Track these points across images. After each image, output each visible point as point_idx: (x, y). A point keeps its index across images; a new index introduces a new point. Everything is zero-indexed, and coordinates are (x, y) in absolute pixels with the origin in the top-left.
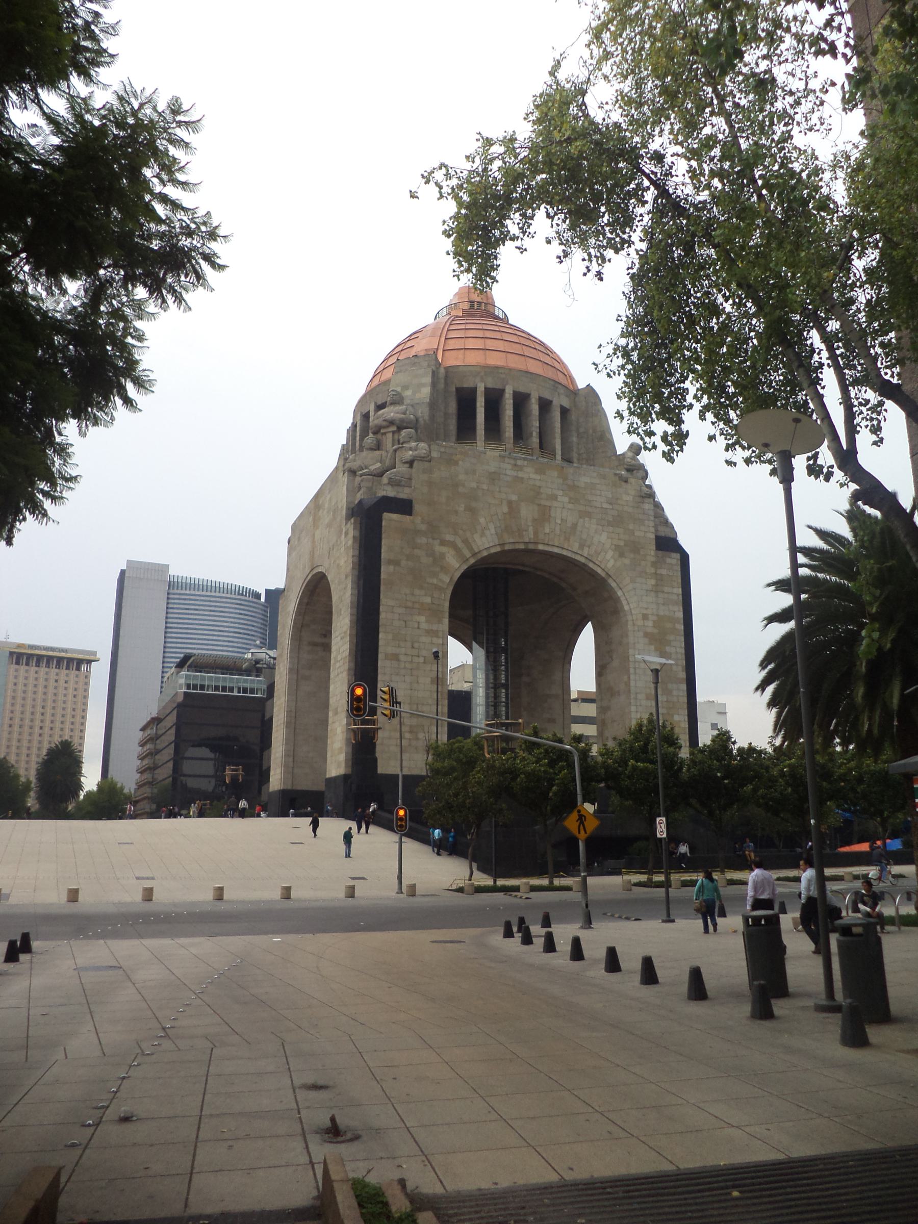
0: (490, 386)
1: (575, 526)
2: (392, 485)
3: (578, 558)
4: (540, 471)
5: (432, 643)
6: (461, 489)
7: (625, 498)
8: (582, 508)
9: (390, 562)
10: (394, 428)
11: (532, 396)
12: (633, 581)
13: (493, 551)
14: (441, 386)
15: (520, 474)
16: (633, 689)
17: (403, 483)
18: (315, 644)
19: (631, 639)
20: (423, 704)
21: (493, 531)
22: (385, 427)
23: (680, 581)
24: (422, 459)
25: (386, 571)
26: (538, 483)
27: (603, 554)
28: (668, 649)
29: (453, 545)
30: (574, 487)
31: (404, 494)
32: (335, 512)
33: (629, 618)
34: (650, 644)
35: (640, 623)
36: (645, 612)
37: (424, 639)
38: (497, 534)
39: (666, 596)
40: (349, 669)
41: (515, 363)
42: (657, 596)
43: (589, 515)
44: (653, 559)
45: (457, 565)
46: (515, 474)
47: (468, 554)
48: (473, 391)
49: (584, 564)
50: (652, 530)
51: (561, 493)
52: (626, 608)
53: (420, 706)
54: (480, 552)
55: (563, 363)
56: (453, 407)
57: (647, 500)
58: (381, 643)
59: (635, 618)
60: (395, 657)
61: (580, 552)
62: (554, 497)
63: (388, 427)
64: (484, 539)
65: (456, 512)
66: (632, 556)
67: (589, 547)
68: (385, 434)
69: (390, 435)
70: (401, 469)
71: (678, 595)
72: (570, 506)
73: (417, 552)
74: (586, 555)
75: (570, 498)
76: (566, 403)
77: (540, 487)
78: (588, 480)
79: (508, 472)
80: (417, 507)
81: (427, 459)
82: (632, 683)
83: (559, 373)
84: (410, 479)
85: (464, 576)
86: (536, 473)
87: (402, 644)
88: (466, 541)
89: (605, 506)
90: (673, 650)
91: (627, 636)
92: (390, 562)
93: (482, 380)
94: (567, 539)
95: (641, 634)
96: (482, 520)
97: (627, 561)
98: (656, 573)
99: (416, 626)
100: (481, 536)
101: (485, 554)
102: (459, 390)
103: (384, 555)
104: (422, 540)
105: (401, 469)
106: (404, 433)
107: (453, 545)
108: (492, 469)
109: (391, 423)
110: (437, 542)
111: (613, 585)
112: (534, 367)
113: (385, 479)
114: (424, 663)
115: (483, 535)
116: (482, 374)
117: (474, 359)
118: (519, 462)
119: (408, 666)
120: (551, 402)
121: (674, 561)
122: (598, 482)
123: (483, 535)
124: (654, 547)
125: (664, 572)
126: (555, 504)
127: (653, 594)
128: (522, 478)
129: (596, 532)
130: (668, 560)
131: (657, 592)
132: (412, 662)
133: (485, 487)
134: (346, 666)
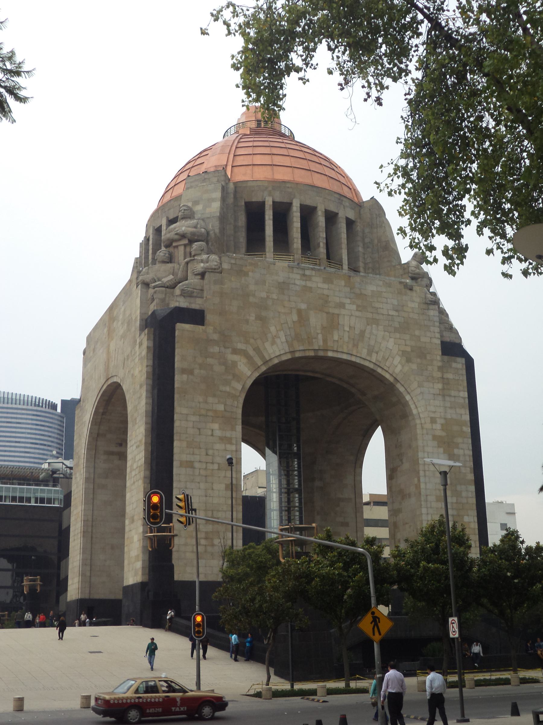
0: (277, 200)
1: (362, 333)
2: (184, 296)
3: (367, 364)
4: (328, 280)
5: (226, 450)
6: (251, 299)
7: (411, 305)
8: (370, 315)
9: (184, 371)
10: (186, 241)
11: (319, 208)
12: (420, 385)
13: (284, 358)
14: (231, 200)
15: (309, 284)
16: (423, 492)
17: (195, 294)
18: (112, 453)
19: (420, 443)
20: (218, 511)
21: (283, 339)
22: (176, 241)
23: (465, 384)
24: (213, 270)
25: (179, 379)
26: (326, 292)
27: (390, 359)
28: (456, 451)
30: (361, 296)
31: (196, 304)
32: (129, 324)
33: (418, 421)
34: (439, 447)
35: (428, 426)
36: (433, 415)
37: (218, 446)
38: (287, 341)
39: (453, 399)
40: (145, 477)
41: (301, 177)
42: (444, 400)
43: (376, 322)
44: (440, 364)
45: (249, 373)
46: (303, 283)
47: (260, 363)
48: (262, 205)
49: (372, 370)
50: (438, 335)
51: (348, 301)
52: (415, 412)
53: (215, 513)
54: (271, 359)
55: (348, 177)
56: (242, 220)
57: (431, 307)
58: (176, 450)
59: (423, 422)
60: (190, 465)
61: (368, 358)
62: (342, 305)
64: (275, 347)
65: (247, 321)
66: (419, 360)
67: (377, 353)
68: (177, 247)
69: (182, 249)
70: (193, 280)
72: (358, 314)
73: (210, 360)
74: (374, 361)
75: (358, 306)
76: (351, 215)
77: (328, 296)
78: (374, 288)
79: (298, 282)
80: (209, 317)
81: (217, 270)
82: (422, 486)
83: (343, 186)
84: (202, 290)
85: (256, 383)
86: (324, 282)
87: (197, 451)
88: (257, 350)
89: (392, 313)
90: (461, 452)
91: (416, 439)
92: (184, 371)
93: (270, 195)
94: (356, 346)
95: (430, 437)
96: (273, 329)
97: (414, 367)
98: (443, 378)
99: (210, 433)
101: (276, 361)
102: (246, 203)
103: (178, 365)
104: (216, 349)
105: (193, 280)
106: (195, 245)
108: (281, 279)
109: (183, 236)
110: (229, 351)
111: (402, 389)
112: (319, 181)
113: (177, 291)
114: (219, 469)
115: (273, 343)
116: (270, 189)
117: (261, 174)
118: (308, 272)
119: (203, 472)
120: (337, 214)
121: (459, 366)
122: (384, 290)
123: (273, 343)
124: (440, 353)
125: (450, 376)
126: (343, 312)
127: (440, 398)
128: (311, 288)
129: (383, 338)
130: (454, 365)
131: (444, 396)
133: (275, 296)
134: (142, 474)
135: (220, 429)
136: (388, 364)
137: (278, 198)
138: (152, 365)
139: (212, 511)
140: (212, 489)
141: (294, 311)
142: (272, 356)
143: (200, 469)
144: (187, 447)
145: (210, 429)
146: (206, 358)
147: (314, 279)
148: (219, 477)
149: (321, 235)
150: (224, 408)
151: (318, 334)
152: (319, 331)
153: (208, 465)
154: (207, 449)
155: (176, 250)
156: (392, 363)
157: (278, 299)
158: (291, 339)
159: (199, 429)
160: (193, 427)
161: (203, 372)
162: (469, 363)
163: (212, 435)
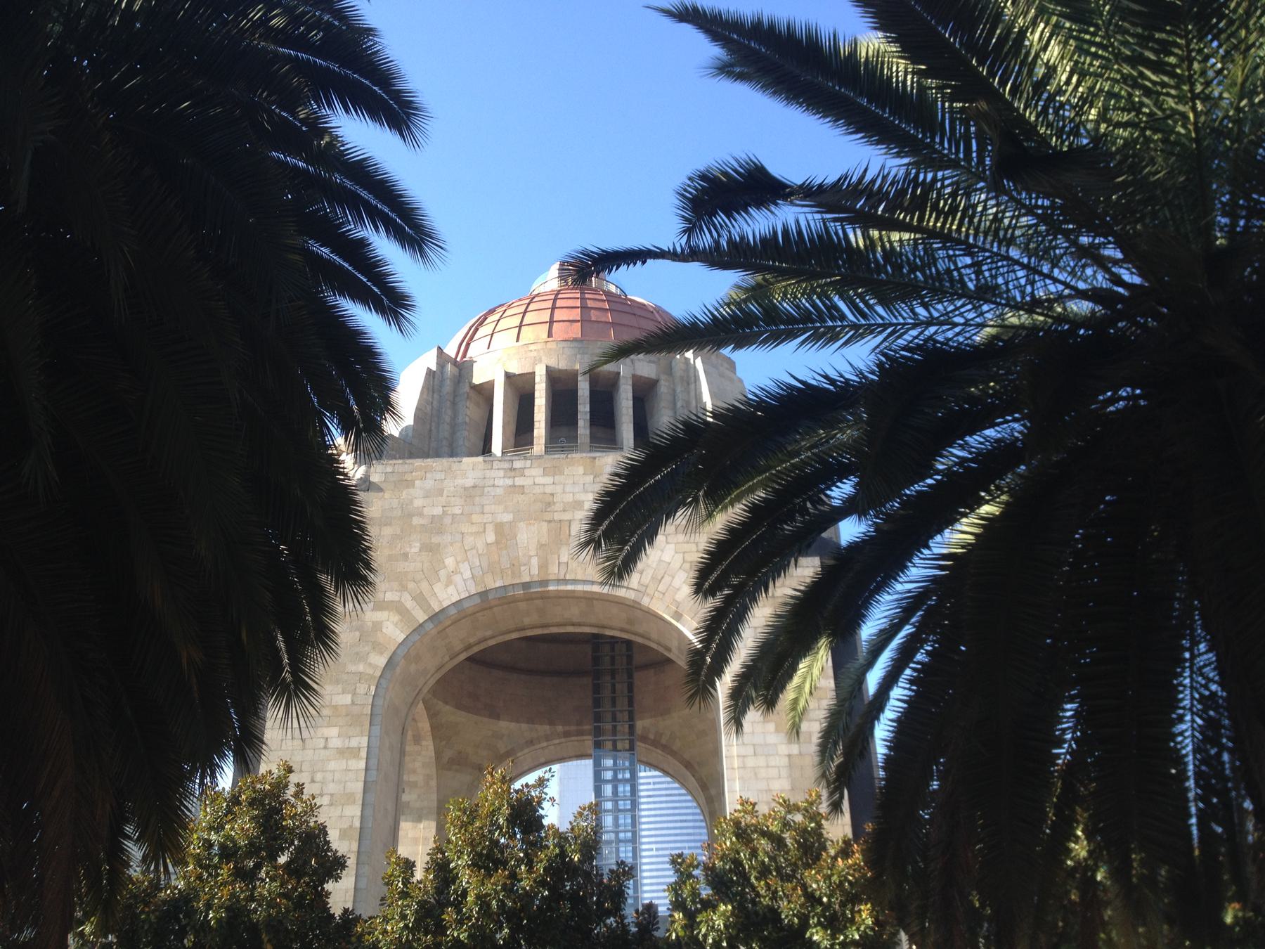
6: (416, 521)
15: (519, 481)
21: (467, 574)
26: (549, 490)
27: (667, 579)
29: (398, 608)
46: (509, 482)
64: (451, 590)
65: (405, 556)
79: (500, 482)
86: (545, 475)
88: (420, 599)
96: (450, 562)
99: (322, 745)
100: (447, 586)
108: (469, 482)
114: (331, 804)
115: (449, 582)
133: (457, 511)
136: (661, 588)
137: (516, 369)
141: (490, 528)
142: (445, 604)
147: (527, 472)
149: (584, 408)
152: (533, 553)
156: (670, 585)
157: (462, 514)
158: (481, 573)
163: (325, 748)
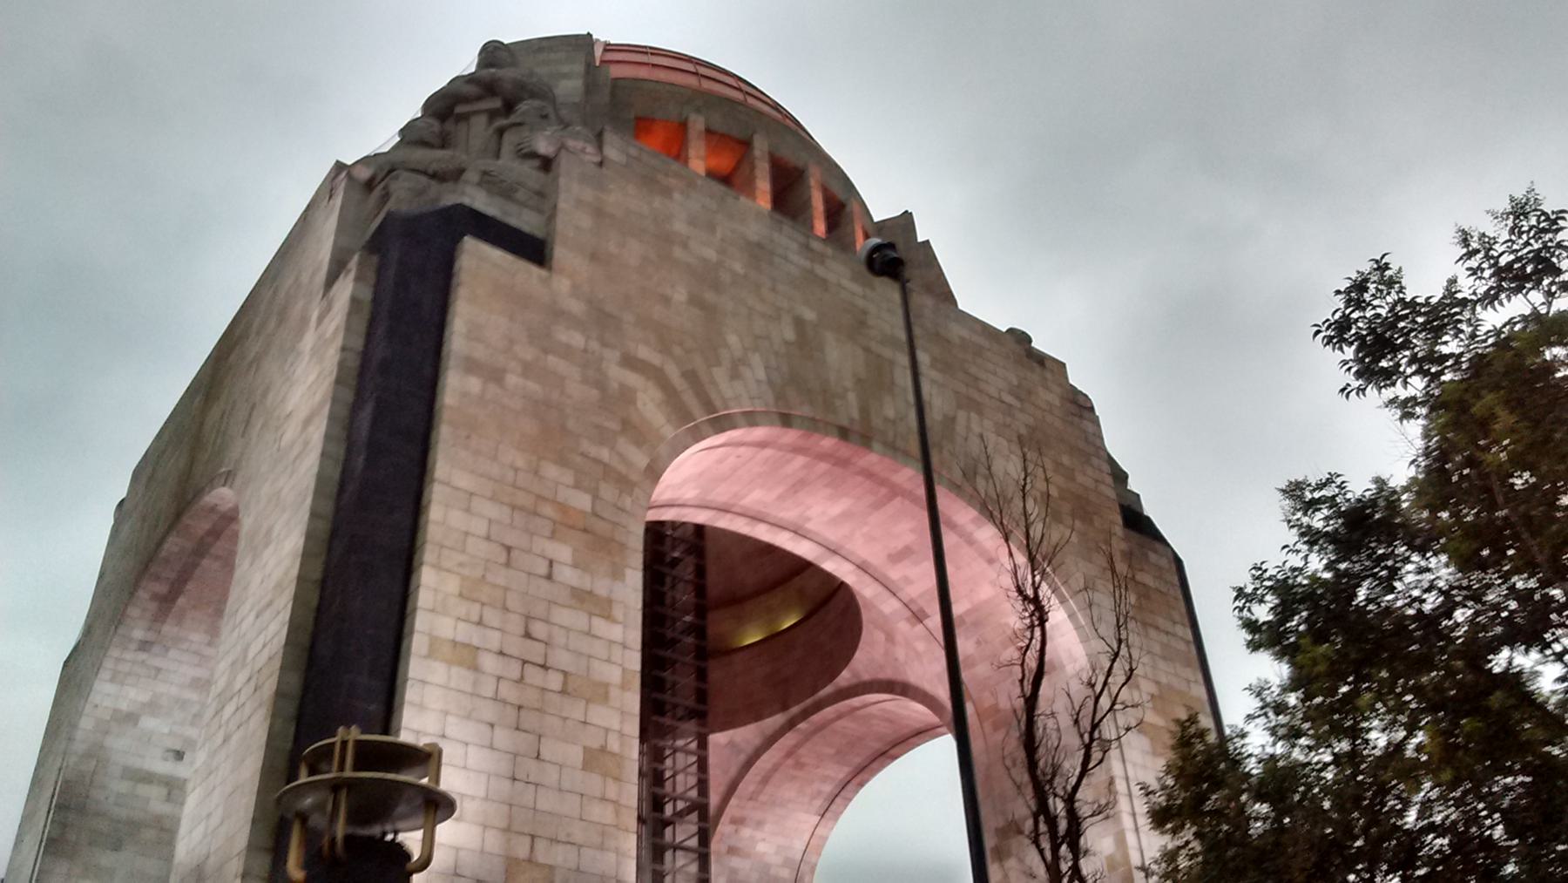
8: (963, 389)
10: (496, 103)
15: (820, 270)
20: (554, 841)
25: (456, 387)
26: (861, 303)
37: (564, 616)
38: (770, 382)
40: (279, 694)
46: (807, 264)
53: (541, 845)
63: (479, 98)
65: (666, 300)
71: (1188, 642)
89: (1009, 399)
92: (471, 366)
96: (733, 339)
99: (542, 569)
107: (658, 376)
114: (563, 692)
119: (508, 691)
123: (735, 375)
132: (521, 680)
133: (738, 267)
134: (270, 686)
135: (575, 566)
138: (361, 349)
139: (533, 837)
140: (538, 757)
143: (499, 678)
144: (461, 595)
145: (544, 557)
146: (546, 351)
148: (565, 719)
150: (593, 508)
151: (846, 390)
152: (849, 383)
153: (529, 669)
154: (528, 618)
155: (462, 127)
159: (509, 549)
160: (488, 538)
161: (532, 386)
162: (1178, 563)
